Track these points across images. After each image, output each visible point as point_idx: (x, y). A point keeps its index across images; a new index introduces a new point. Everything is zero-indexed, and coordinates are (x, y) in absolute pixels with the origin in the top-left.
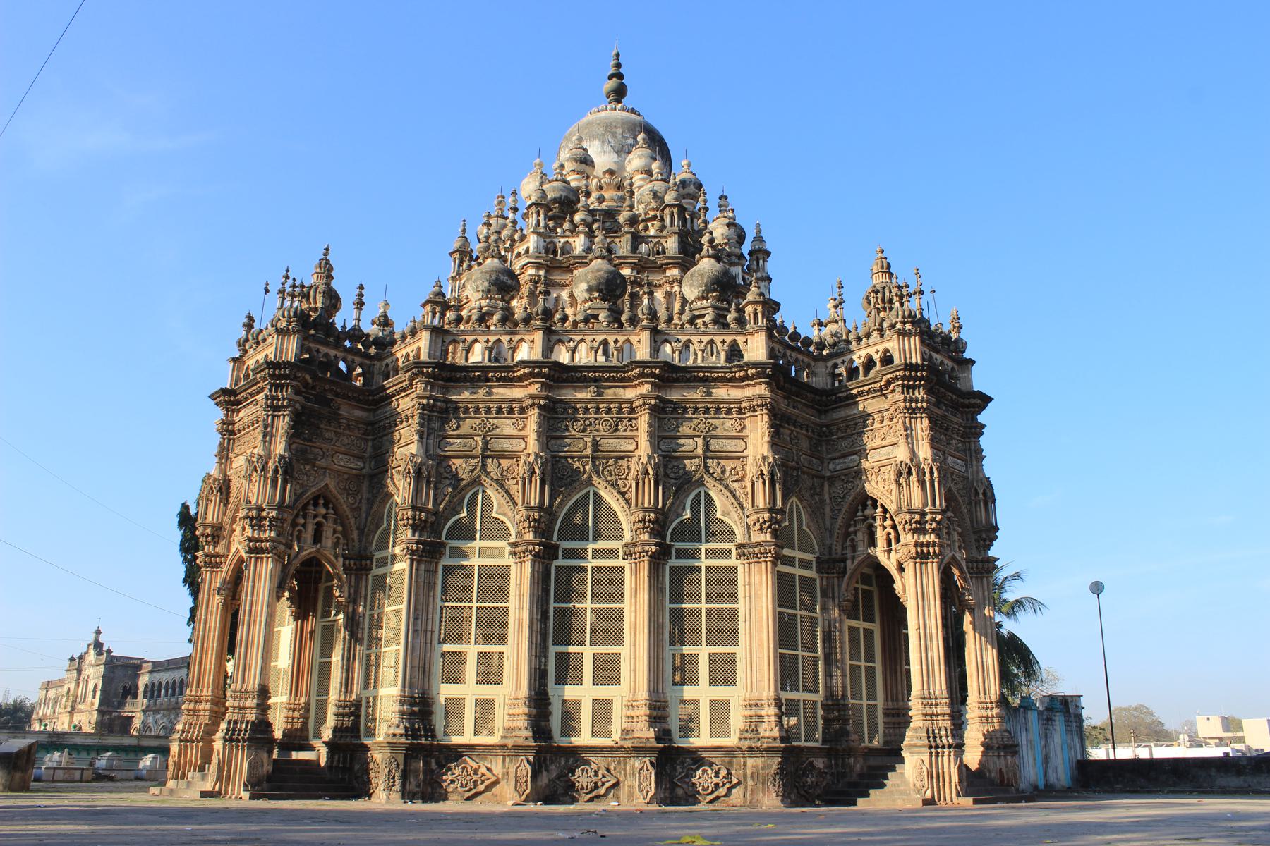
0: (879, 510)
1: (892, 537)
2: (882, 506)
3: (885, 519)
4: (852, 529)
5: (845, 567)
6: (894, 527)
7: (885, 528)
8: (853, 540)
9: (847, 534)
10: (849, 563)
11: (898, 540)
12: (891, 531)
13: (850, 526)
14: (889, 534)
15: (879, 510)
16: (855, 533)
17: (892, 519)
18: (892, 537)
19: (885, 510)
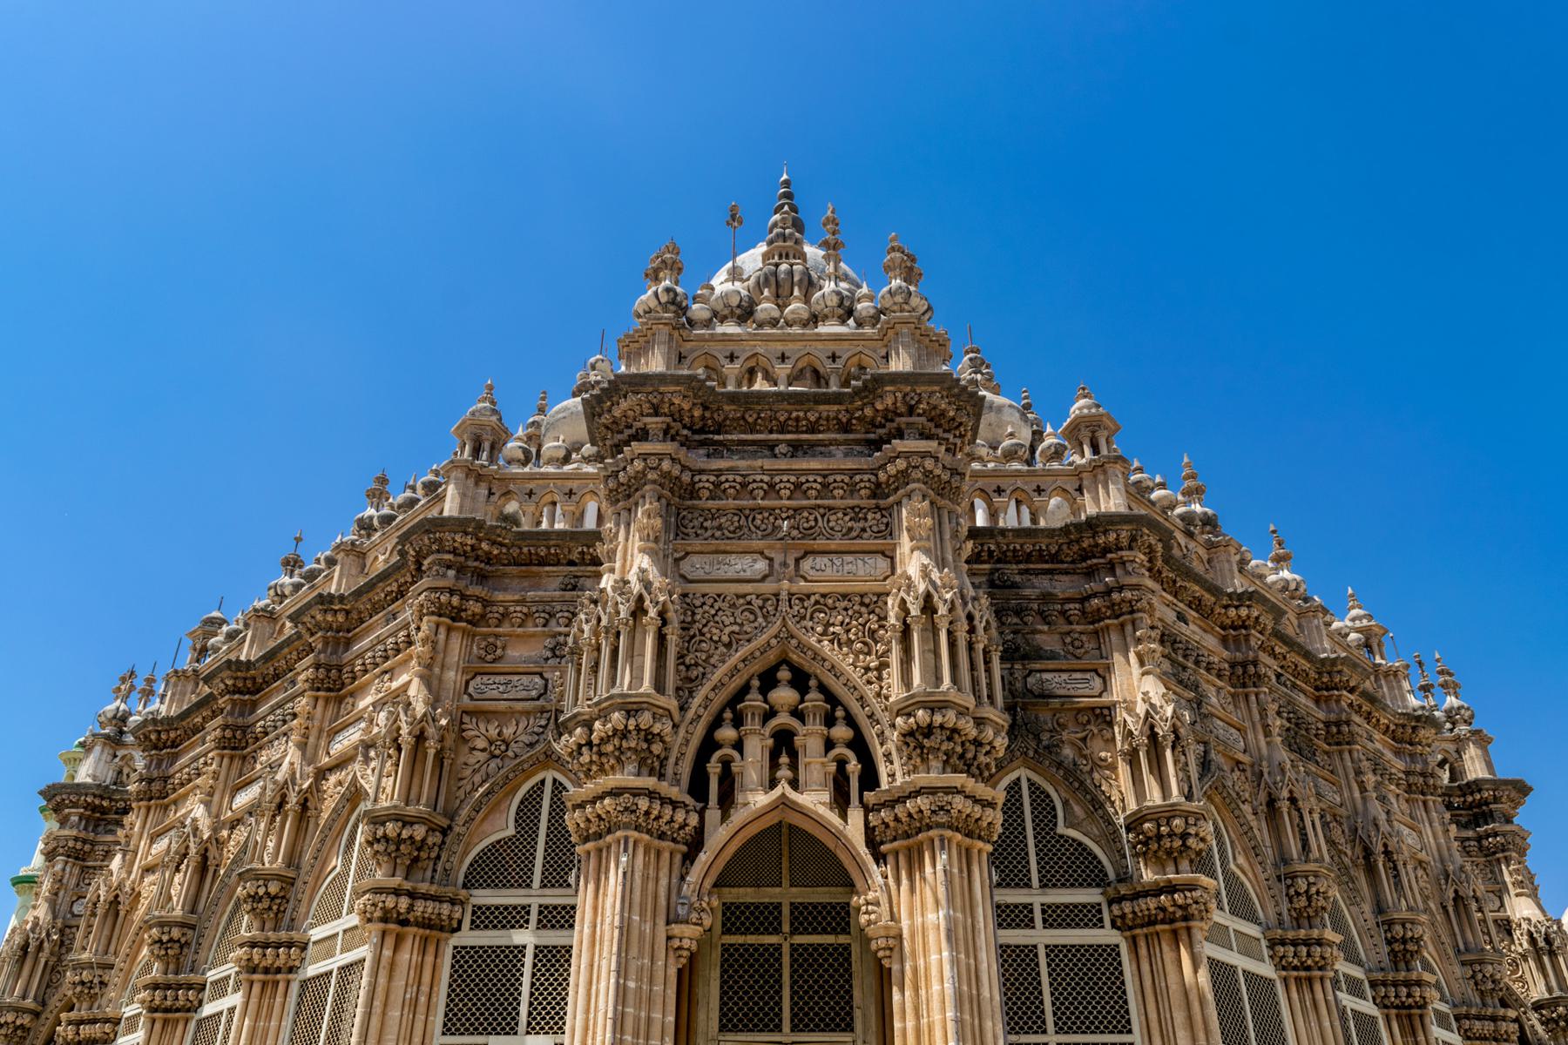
0: (814, 695)
1: (854, 767)
2: (823, 688)
3: (830, 721)
4: (727, 733)
5: (700, 831)
6: (859, 745)
7: (829, 744)
8: (726, 764)
9: (709, 745)
10: (713, 814)
11: (870, 779)
12: (850, 754)
13: (717, 723)
14: (842, 763)
15: (814, 695)
16: (739, 746)
17: (850, 721)
18: (854, 767)
19: (831, 698)
